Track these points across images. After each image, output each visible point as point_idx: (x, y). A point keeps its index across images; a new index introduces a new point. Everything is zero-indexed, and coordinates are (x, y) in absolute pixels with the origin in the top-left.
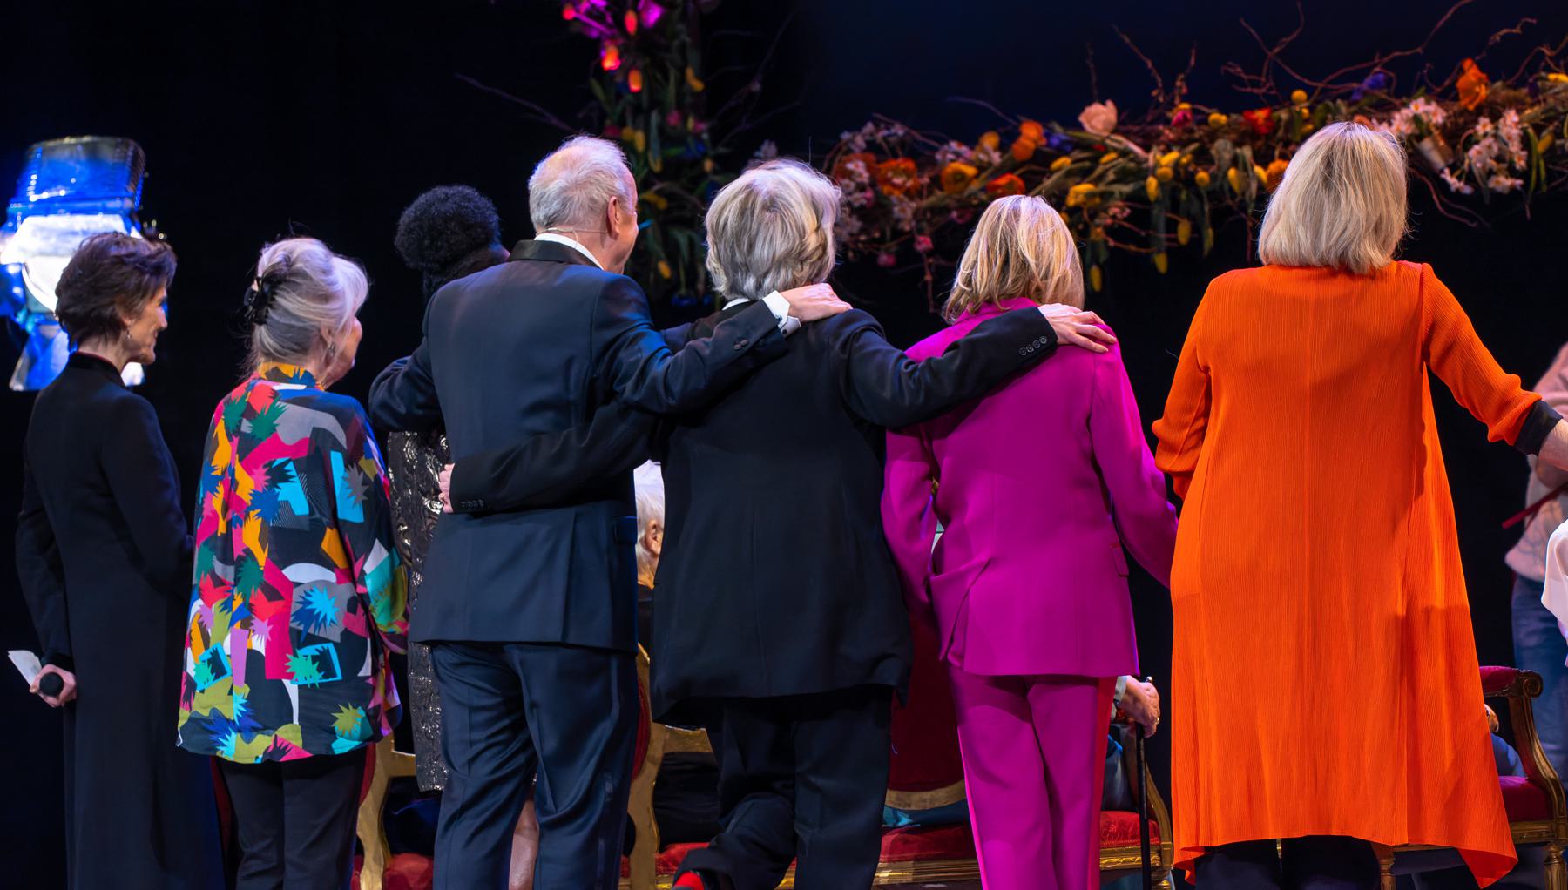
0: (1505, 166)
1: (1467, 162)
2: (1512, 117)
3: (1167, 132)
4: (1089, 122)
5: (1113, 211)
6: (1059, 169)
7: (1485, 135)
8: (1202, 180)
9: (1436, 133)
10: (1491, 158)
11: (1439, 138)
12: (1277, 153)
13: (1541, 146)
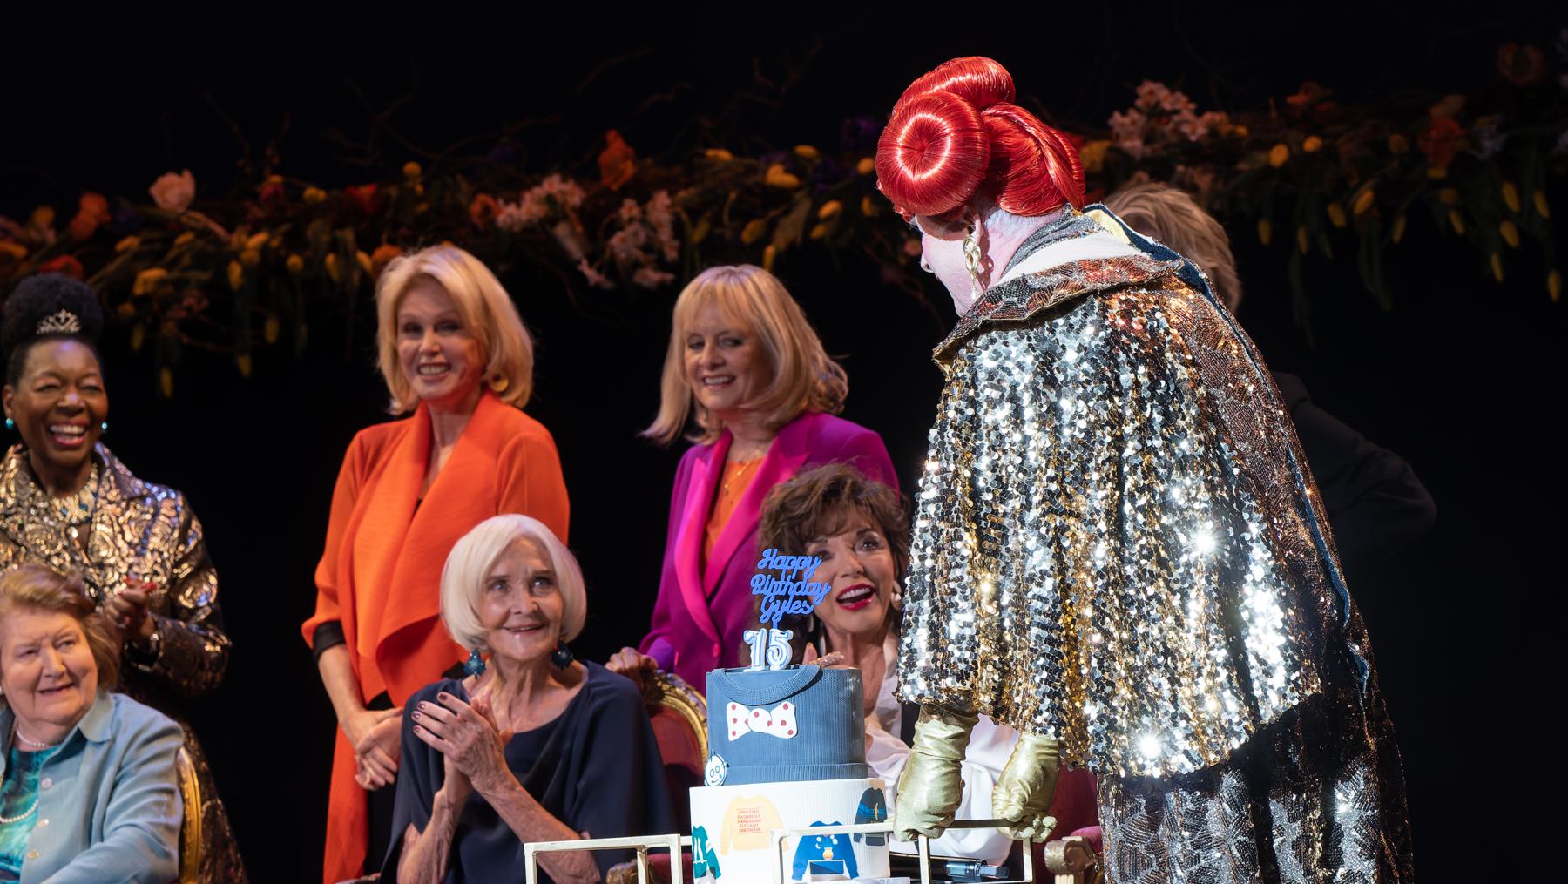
0: (653, 257)
1: (608, 253)
2: (662, 199)
5: (189, 301)
6: (125, 251)
7: (631, 220)
9: (573, 216)
12: (384, 237)
13: (698, 234)
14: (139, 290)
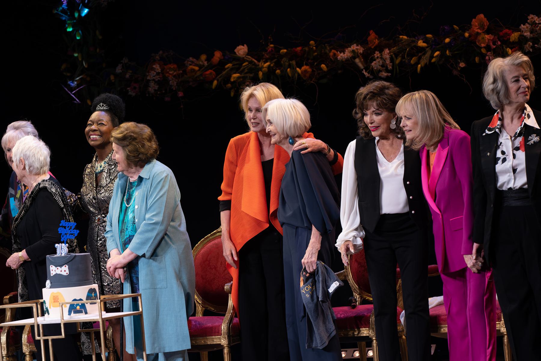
0: (385, 68)
1: (371, 67)
2: (387, 51)
3: (266, 55)
4: (238, 52)
6: (228, 68)
7: (378, 57)
8: (277, 73)
10: (380, 66)
11: (361, 58)
12: (304, 63)
13: (398, 61)
14: (232, 80)
